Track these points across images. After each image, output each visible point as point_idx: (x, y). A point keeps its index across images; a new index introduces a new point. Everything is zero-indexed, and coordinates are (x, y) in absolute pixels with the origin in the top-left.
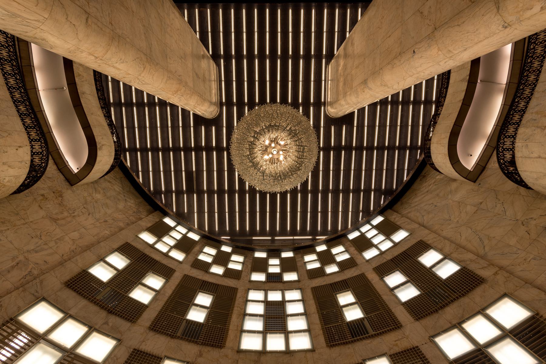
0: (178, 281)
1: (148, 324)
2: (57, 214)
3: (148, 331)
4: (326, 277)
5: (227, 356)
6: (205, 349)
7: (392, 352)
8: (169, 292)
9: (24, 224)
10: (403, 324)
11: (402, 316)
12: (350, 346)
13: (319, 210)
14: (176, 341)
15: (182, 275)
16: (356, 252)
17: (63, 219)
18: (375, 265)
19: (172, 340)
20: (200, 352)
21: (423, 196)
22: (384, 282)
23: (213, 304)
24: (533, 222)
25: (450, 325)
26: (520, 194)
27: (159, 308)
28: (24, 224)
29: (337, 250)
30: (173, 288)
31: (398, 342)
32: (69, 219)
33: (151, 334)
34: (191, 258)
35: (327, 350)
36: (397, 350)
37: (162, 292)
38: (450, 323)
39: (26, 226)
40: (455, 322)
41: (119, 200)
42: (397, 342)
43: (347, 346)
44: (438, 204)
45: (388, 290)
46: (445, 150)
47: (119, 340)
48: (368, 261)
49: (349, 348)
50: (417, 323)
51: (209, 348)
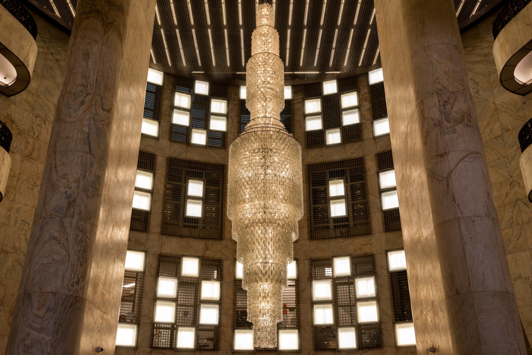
0: (164, 169)
1: (158, 230)
2: (26, 147)
3: (161, 236)
4: (324, 150)
5: (227, 247)
6: (210, 243)
8: (161, 187)
9: (18, 181)
10: (374, 232)
12: (326, 241)
13: (333, 51)
14: (185, 239)
15: (164, 159)
17: (33, 149)
19: (182, 239)
20: (206, 246)
21: (479, 59)
23: (206, 191)
24: (517, 189)
27: (160, 211)
28: (18, 181)
29: (350, 100)
30: (163, 181)
31: (363, 247)
32: (37, 146)
33: (164, 238)
34: (166, 128)
35: (307, 243)
36: (360, 252)
37: (155, 191)
39: (20, 181)
41: (51, 68)
43: (324, 241)
44: (481, 92)
45: (377, 190)
47: (146, 252)
48: (376, 139)
49: (325, 243)
50: (384, 234)
51: (212, 242)
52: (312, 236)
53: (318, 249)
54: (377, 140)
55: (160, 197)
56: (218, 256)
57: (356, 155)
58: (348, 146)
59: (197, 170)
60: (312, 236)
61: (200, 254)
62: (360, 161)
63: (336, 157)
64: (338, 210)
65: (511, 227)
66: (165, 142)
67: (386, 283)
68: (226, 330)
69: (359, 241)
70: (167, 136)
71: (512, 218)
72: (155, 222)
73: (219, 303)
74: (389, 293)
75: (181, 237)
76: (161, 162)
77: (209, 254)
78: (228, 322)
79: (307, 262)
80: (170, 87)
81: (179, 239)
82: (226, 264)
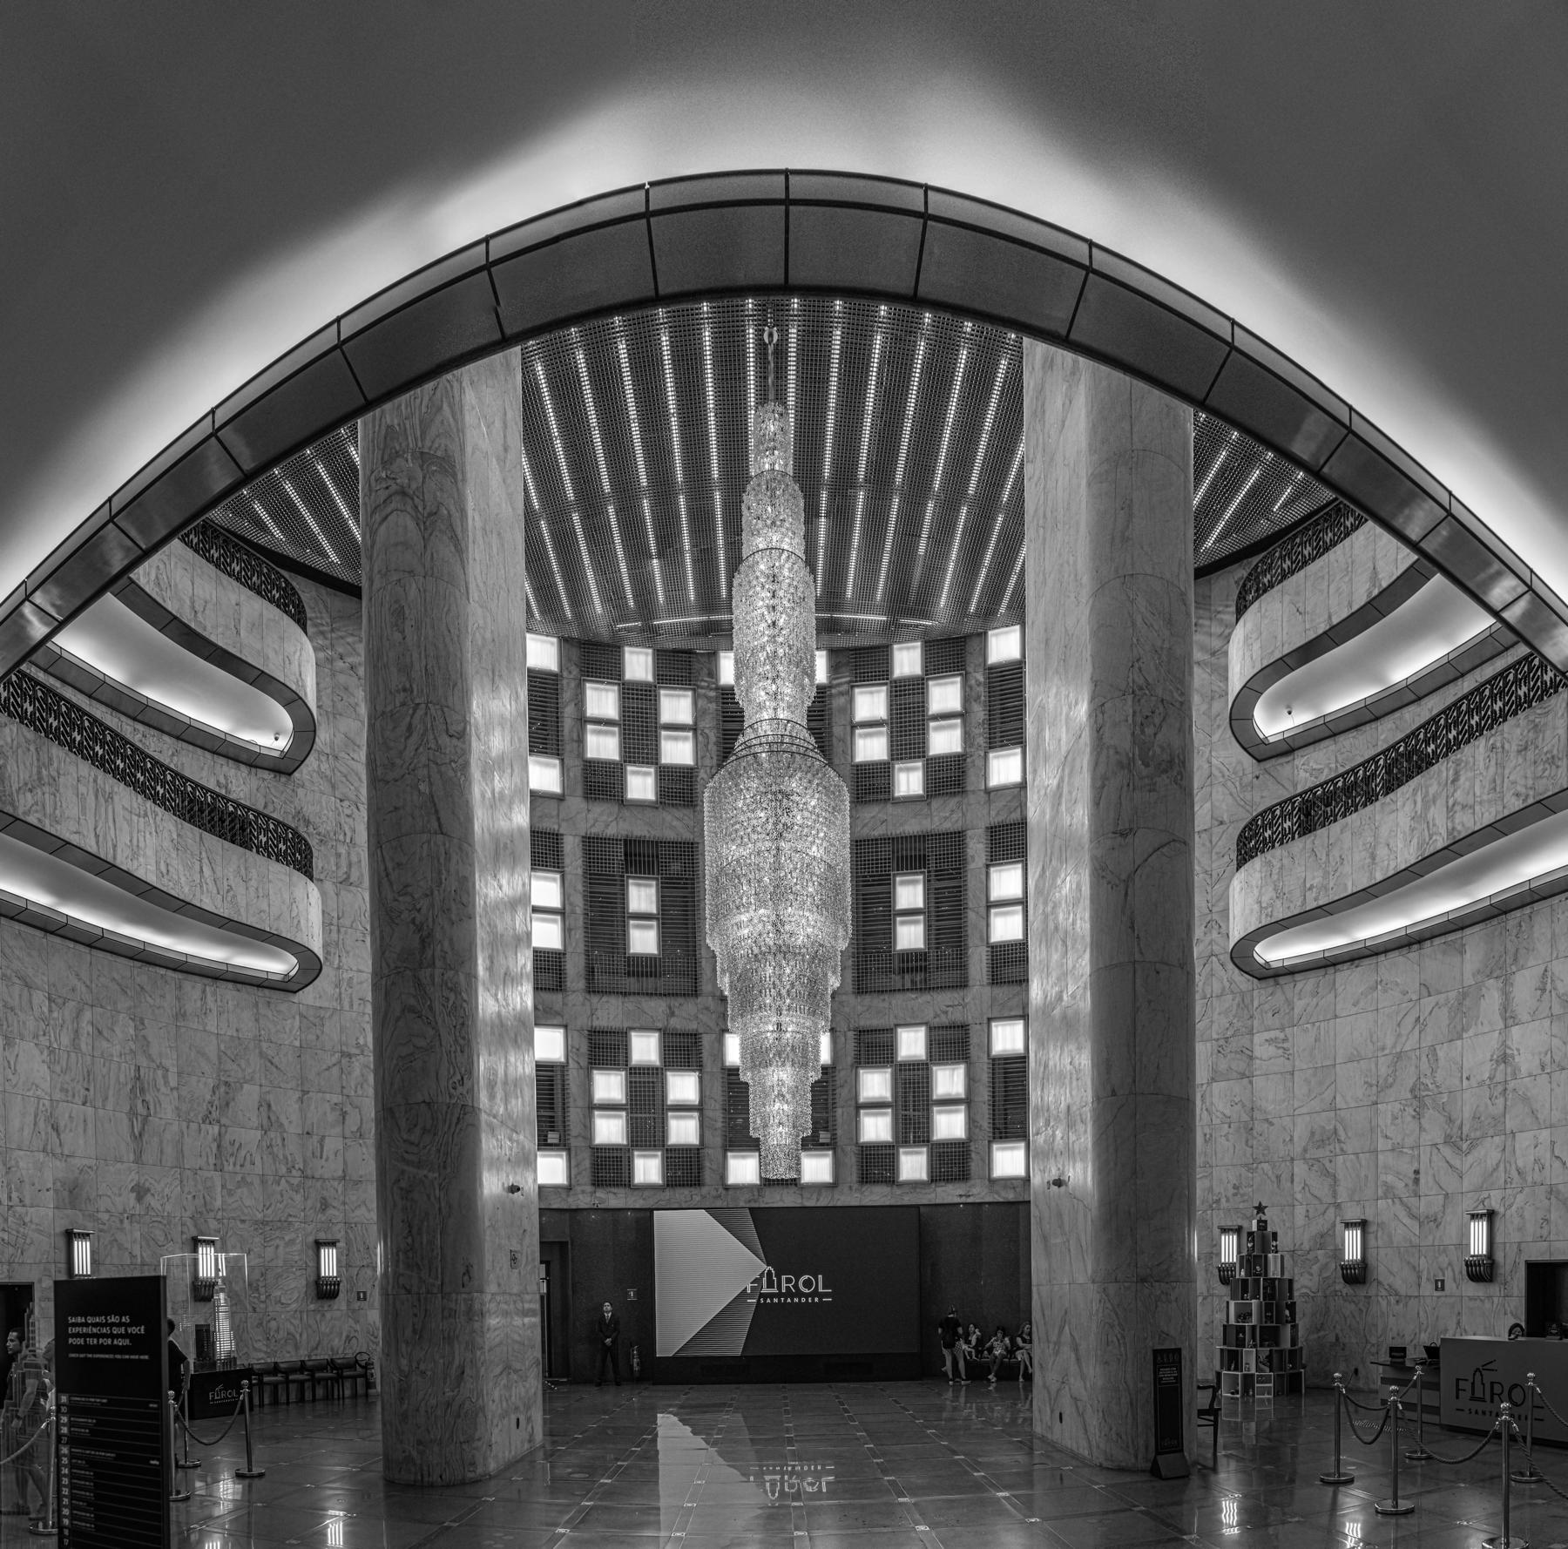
0: (580, 862)
1: (582, 984)
4: (890, 808)
5: (707, 1009)
6: (675, 1002)
7: (936, 1022)
8: (579, 901)
14: (632, 998)
15: (578, 840)
23: (663, 901)
27: (581, 948)
33: (595, 999)
34: (576, 772)
35: (852, 1000)
36: (944, 1020)
50: (988, 989)
51: (681, 1000)
52: (861, 988)
53: (870, 1012)
55: (579, 921)
56: (692, 1026)
57: (947, 826)
59: (640, 857)
60: (861, 988)
61: (660, 1025)
62: (956, 840)
64: (910, 936)
66: (576, 803)
68: (712, 1153)
69: (944, 999)
70: (579, 790)
72: (574, 968)
73: (700, 1108)
75: (625, 994)
76: (572, 848)
77: (676, 1024)
78: (716, 1140)
79: (851, 1034)
80: (575, 671)
81: (621, 998)
82: (706, 1040)
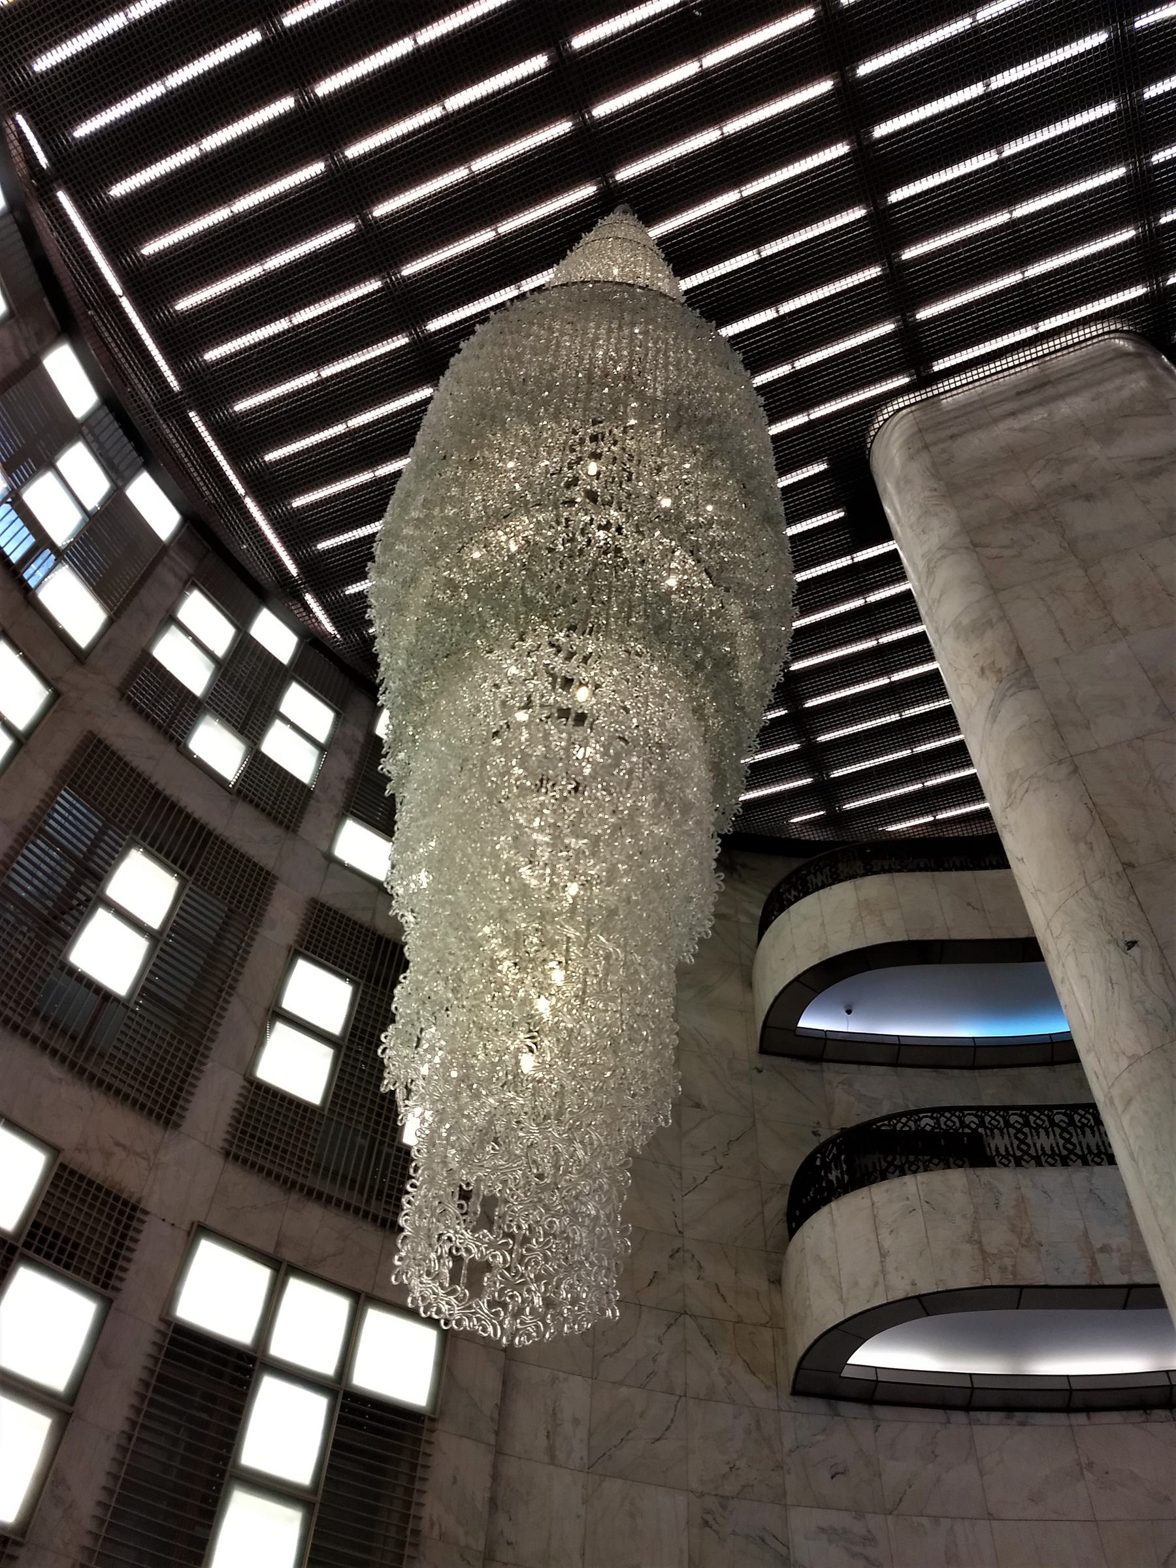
10: (186, 1126)
11: (211, 1106)
16: (338, 792)
18: (334, 895)
22: (289, 967)
25: (270, 1249)
26: (764, 1203)
29: (307, 711)
31: (120, 1154)
36: (94, 1166)
38: (278, 1244)
40: (289, 1255)
42: (116, 1150)
46: (842, 943)
50: (217, 1161)
54: (333, 866)
58: (244, 811)
63: (197, 804)
65: (642, 1387)
67: (136, 1356)
71: (654, 1360)
74: (126, 1412)
